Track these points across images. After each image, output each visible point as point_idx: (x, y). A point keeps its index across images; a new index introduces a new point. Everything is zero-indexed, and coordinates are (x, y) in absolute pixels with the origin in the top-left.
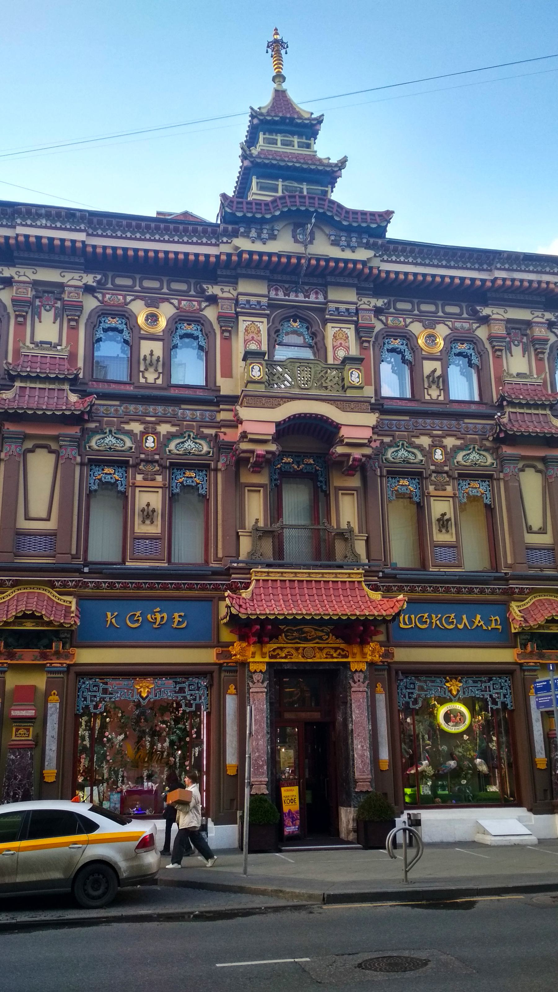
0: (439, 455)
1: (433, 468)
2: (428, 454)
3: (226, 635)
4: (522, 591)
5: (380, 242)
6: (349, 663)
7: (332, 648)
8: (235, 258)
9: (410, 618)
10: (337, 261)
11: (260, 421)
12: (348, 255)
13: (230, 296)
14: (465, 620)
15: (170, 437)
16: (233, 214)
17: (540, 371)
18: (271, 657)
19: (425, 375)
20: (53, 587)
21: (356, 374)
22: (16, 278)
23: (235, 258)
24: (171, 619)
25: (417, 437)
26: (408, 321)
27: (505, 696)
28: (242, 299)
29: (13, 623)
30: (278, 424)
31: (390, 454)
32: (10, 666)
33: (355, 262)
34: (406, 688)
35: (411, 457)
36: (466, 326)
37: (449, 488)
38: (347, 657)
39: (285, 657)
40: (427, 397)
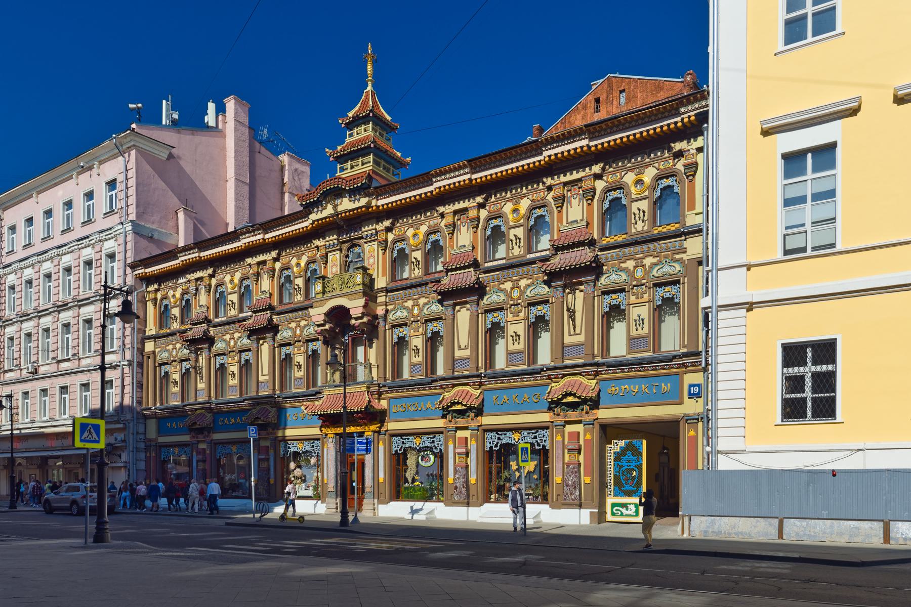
0: (416, 311)
2: (410, 311)
31: (391, 317)
36: (436, 221)
37: (421, 330)
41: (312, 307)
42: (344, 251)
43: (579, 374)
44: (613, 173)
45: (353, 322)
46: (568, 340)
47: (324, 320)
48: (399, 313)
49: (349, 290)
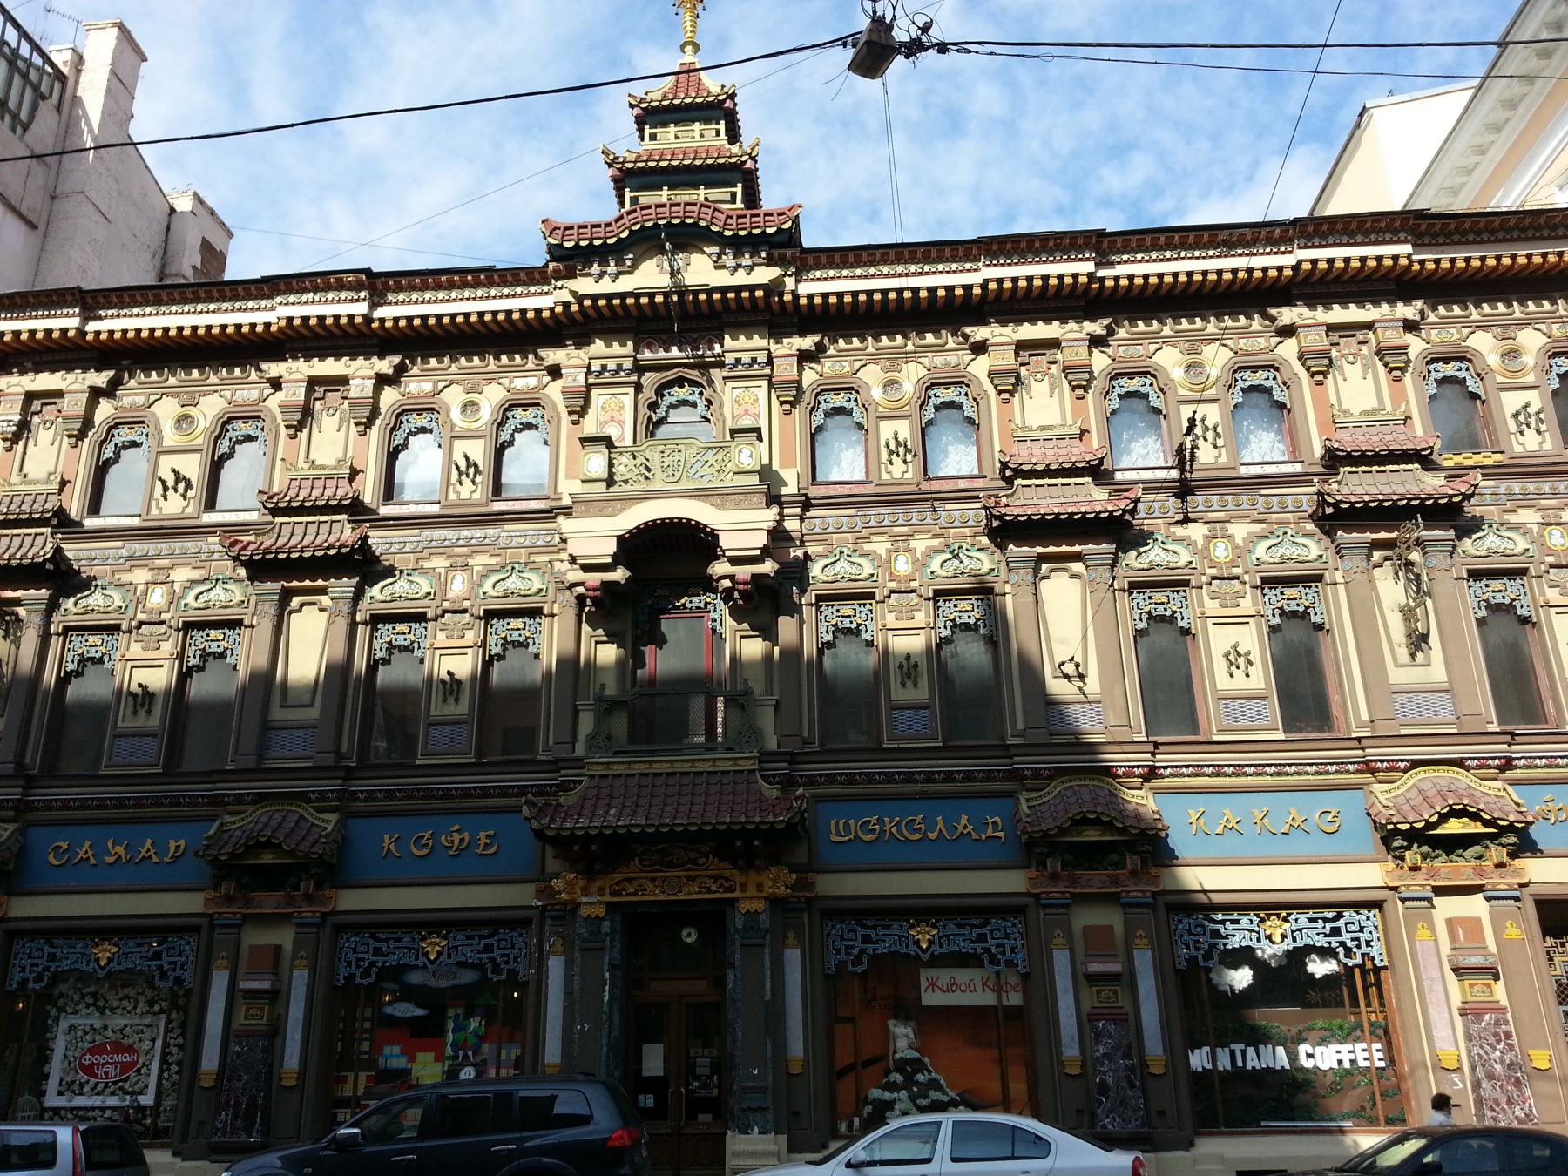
1: (892, 585)
3: (552, 865)
4: (1036, 774)
5: (789, 253)
6: (735, 900)
7: (710, 877)
8: (575, 308)
9: (846, 824)
10: (724, 290)
11: (595, 537)
12: (741, 278)
13: (580, 362)
14: (941, 825)
15: (490, 571)
16: (560, 246)
17: (1080, 413)
18: (612, 895)
19: (883, 443)
20: (308, 801)
21: (746, 451)
22: (286, 377)
23: (575, 308)
24: (474, 841)
25: (867, 539)
26: (857, 364)
27: (1012, 950)
28: (596, 367)
29: (239, 857)
30: (620, 539)
32: (245, 917)
33: (752, 288)
34: (842, 939)
35: (854, 570)
36: (953, 360)
38: (733, 891)
39: (635, 894)
40: (885, 476)
41: (568, 515)
42: (649, 394)
43: (1459, 763)
44: (1445, 324)
45: (720, 568)
46: (1399, 676)
47: (614, 556)
48: (843, 567)
49: (704, 483)
